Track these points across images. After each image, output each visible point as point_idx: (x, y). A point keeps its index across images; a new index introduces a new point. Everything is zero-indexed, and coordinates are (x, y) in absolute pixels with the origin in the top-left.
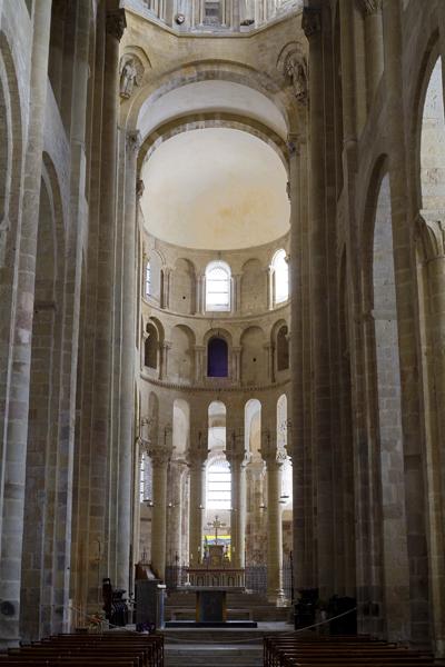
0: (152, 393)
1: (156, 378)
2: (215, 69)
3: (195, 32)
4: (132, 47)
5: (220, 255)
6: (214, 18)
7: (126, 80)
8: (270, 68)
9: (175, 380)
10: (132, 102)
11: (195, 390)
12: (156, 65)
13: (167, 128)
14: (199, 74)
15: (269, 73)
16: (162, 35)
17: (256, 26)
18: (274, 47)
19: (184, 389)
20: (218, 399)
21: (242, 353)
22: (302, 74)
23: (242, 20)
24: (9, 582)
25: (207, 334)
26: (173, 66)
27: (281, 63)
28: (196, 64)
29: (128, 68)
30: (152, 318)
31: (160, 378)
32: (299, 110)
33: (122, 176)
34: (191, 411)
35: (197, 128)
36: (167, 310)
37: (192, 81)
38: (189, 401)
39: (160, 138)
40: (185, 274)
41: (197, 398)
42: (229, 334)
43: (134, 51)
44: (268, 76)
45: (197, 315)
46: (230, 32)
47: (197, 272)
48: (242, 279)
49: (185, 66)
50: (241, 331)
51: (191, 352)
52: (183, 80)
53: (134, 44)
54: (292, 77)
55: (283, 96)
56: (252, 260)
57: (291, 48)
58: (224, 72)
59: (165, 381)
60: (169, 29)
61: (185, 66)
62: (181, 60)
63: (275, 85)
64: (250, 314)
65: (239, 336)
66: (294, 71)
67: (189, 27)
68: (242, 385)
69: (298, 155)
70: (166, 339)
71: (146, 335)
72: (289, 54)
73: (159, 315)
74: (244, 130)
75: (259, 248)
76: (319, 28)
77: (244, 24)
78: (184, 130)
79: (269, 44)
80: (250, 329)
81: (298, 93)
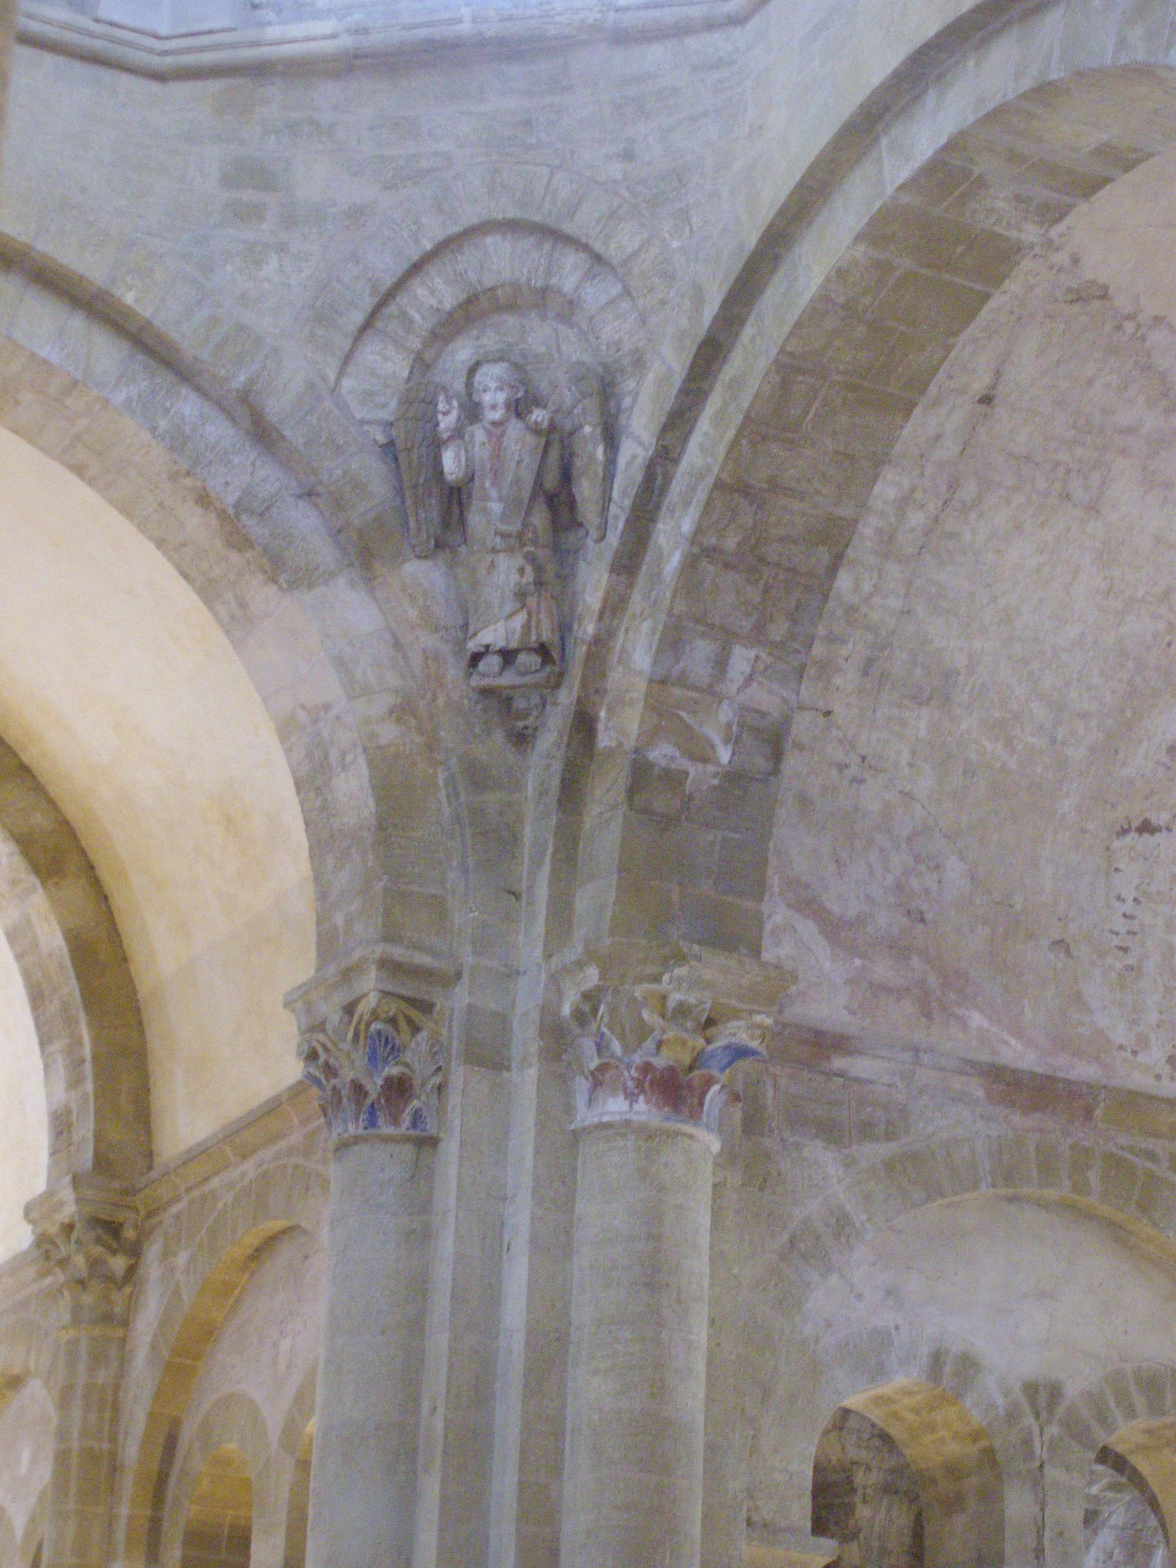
15: (275, 407)
18: (357, 214)
22: (557, 501)
27: (385, 362)
32: (477, 777)
44: (262, 434)
54: (456, 499)
55: (352, 632)
57: (501, 261)
63: (306, 523)
66: (491, 456)
79: (315, 178)
81: (494, 634)
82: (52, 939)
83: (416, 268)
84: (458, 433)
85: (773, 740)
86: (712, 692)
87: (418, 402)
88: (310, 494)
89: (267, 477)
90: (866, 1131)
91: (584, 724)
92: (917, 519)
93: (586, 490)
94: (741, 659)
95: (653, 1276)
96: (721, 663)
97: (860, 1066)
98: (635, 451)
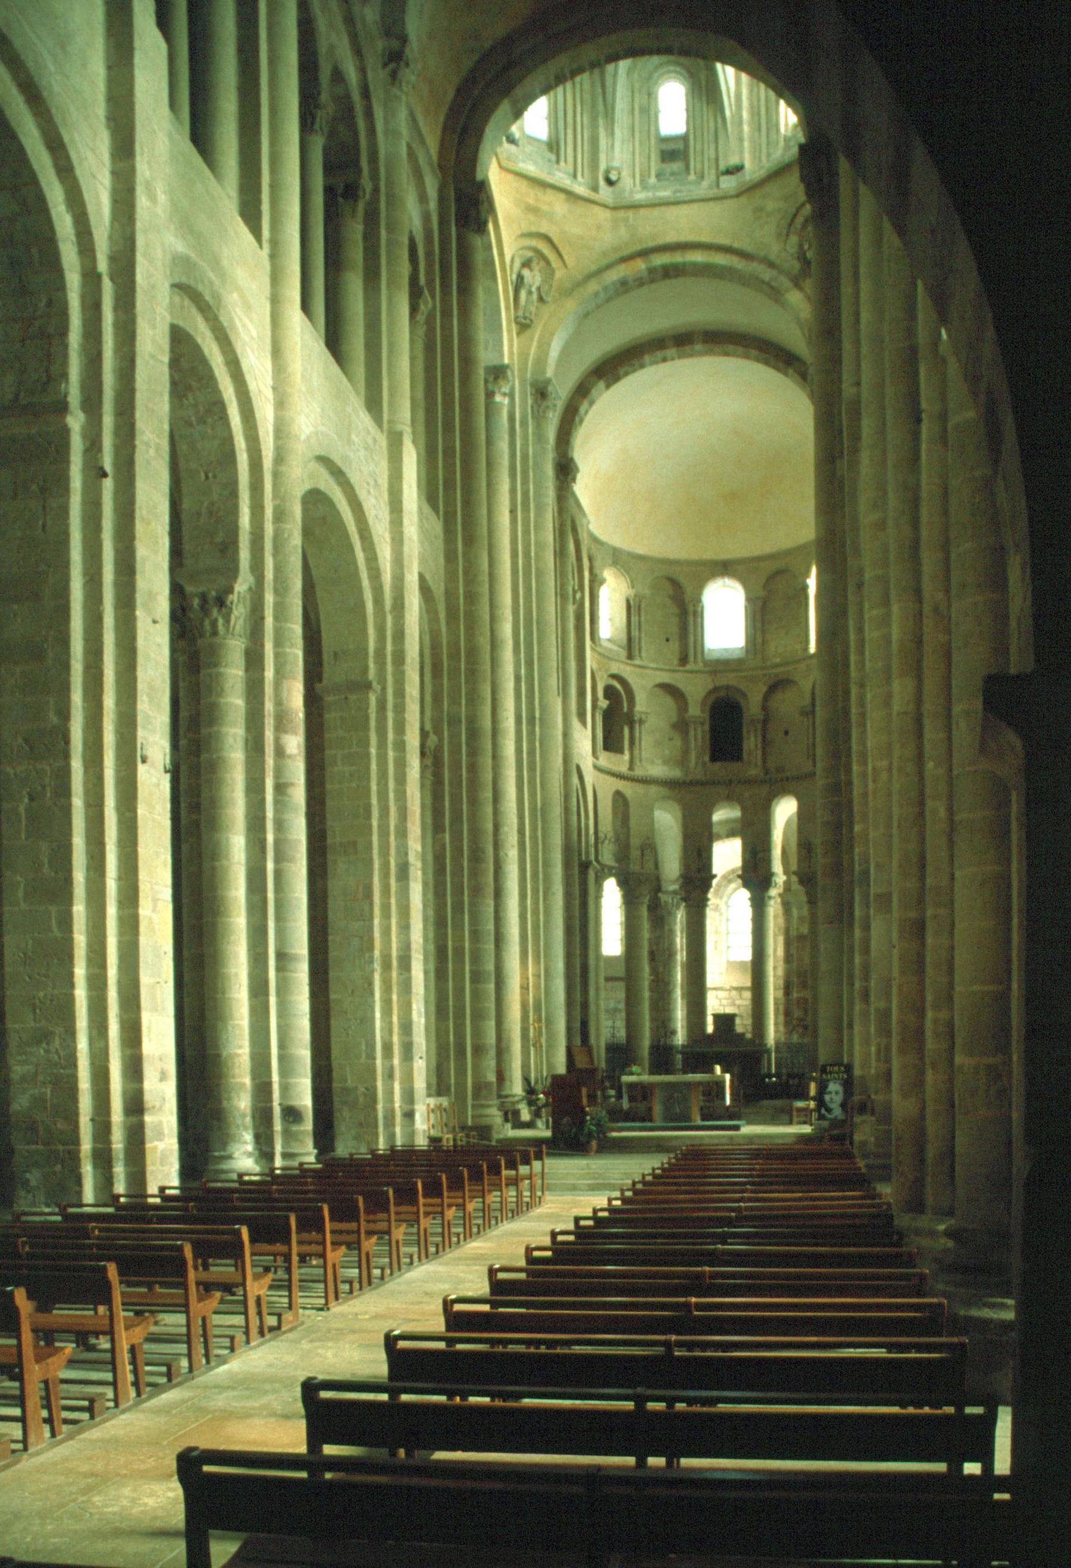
0: (618, 794)
1: (624, 769)
2: (678, 258)
3: (640, 196)
5: (724, 568)
6: (676, 166)
9: (658, 770)
10: (537, 333)
11: (691, 783)
13: (610, 369)
19: (671, 784)
20: (729, 799)
21: (765, 722)
24: (297, 1080)
25: (710, 693)
26: (605, 262)
28: (644, 253)
30: (614, 676)
31: (631, 768)
34: (684, 816)
35: (664, 360)
36: (637, 662)
37: (640, 282)
38: (679, 801)
39: (601, 384)
40: (668, 602)
41: (693, 796)
42: (745, 695)
45: (688, 667)
46: (704, 188)
47: (689, 591)
48: (764, 604)
49: (624, 260)
50: (764, 689)
51: (681, 726)
56: (779, 572)
59: (638, 772)
61: (624, 260)
62: (616, 249)
64: (778, 660)
65: (761, 696)
67: (631, 188)
68: (767, 773)
70: (638, 708)
71: (604, 703)
73: (626, 671)
75: (788, 553)
78: (642, 366)
80: (777, 685)
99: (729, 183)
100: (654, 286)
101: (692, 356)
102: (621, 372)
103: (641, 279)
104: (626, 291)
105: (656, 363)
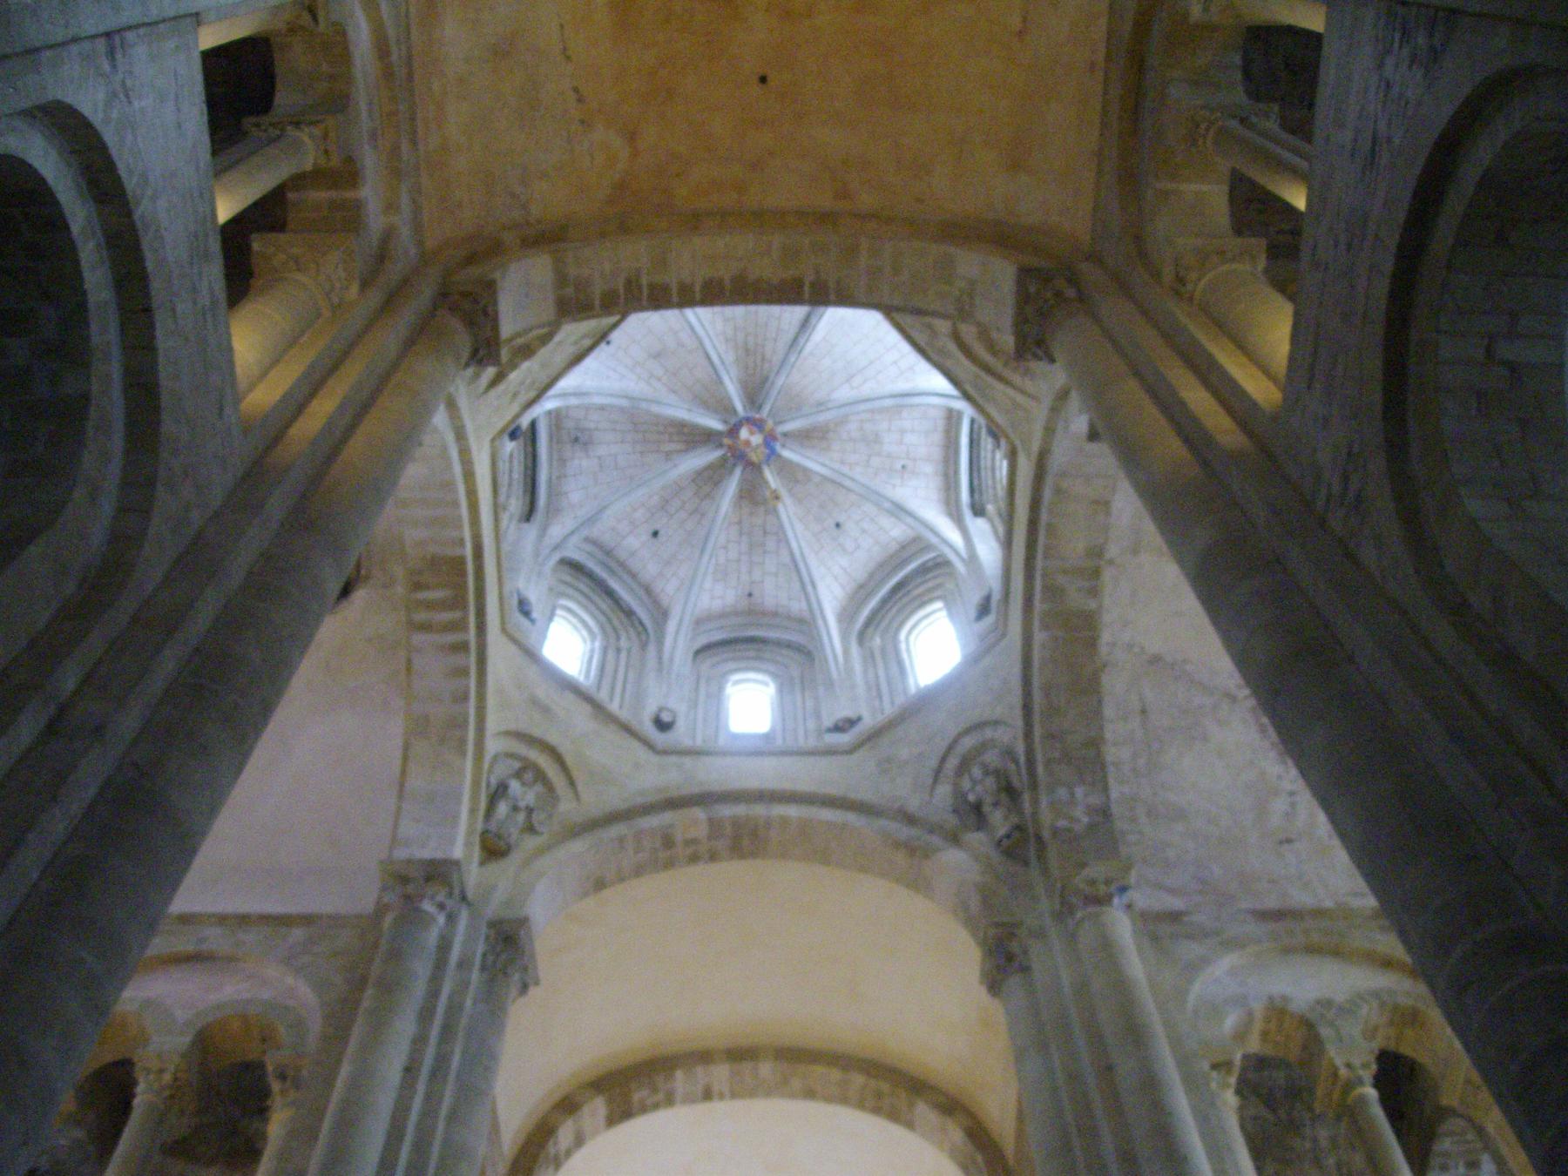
4: (531, 741)
7: (502, 808)
8: (914, 804)
12: (594, 800)
14: (715, 825)
16: (612, 735)
17: (869, 721)
23: (828, 722)
29: (515, 785)
33: (454, 1009)
35: (708, 1095)
43: (534, 755)
44: (910, 819)
52: (668, 842)
53: (537, 732)
54: (977, 808)
57: (968, 742)
58: (784, 821)
60: (634, 724)
66: (980, 787)
69: (1025, 969)
72: (964, 767)
74: (844, 1100)
76: (1070, 293)
77: (838, 728)
78: (669, 1101)
81: (1002, 831)
82: (957, 1135)
83: (943, 760)
84: (972, 789)
85: (1105, 813)
86: (1072, 801)
87: (959, 795)
88: (931, 832)
89: (915, 832)
90: (1206, 935)
91: (1039, 838)
92: (1142, 762)
93: (1016, 782)
94: (1079, 792)
95: (1106, 945)
96: (1072, 795)
97: (1197, 918)
98: (1022, 759)
99: (844, 739)
100: (714, 868)
101: (752, 1093)
102: (636, 1097)
103: (694, 841)
104: (669, 864)
105: (690, 1100)
